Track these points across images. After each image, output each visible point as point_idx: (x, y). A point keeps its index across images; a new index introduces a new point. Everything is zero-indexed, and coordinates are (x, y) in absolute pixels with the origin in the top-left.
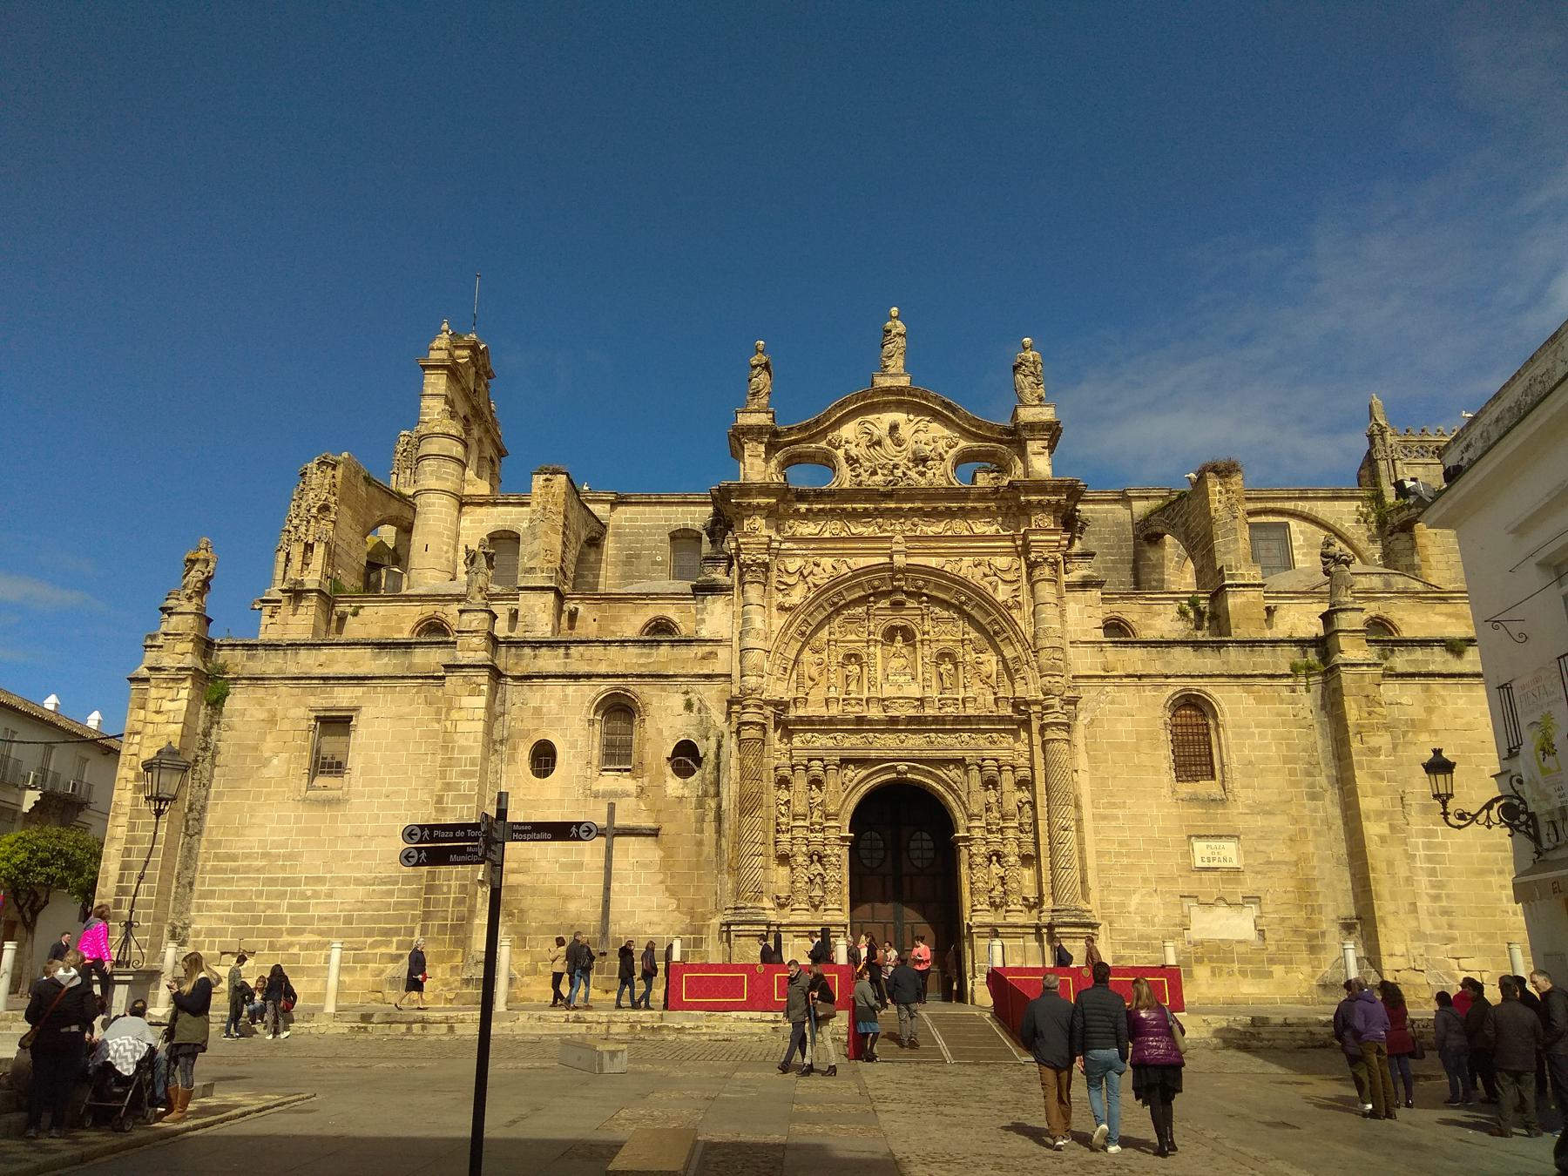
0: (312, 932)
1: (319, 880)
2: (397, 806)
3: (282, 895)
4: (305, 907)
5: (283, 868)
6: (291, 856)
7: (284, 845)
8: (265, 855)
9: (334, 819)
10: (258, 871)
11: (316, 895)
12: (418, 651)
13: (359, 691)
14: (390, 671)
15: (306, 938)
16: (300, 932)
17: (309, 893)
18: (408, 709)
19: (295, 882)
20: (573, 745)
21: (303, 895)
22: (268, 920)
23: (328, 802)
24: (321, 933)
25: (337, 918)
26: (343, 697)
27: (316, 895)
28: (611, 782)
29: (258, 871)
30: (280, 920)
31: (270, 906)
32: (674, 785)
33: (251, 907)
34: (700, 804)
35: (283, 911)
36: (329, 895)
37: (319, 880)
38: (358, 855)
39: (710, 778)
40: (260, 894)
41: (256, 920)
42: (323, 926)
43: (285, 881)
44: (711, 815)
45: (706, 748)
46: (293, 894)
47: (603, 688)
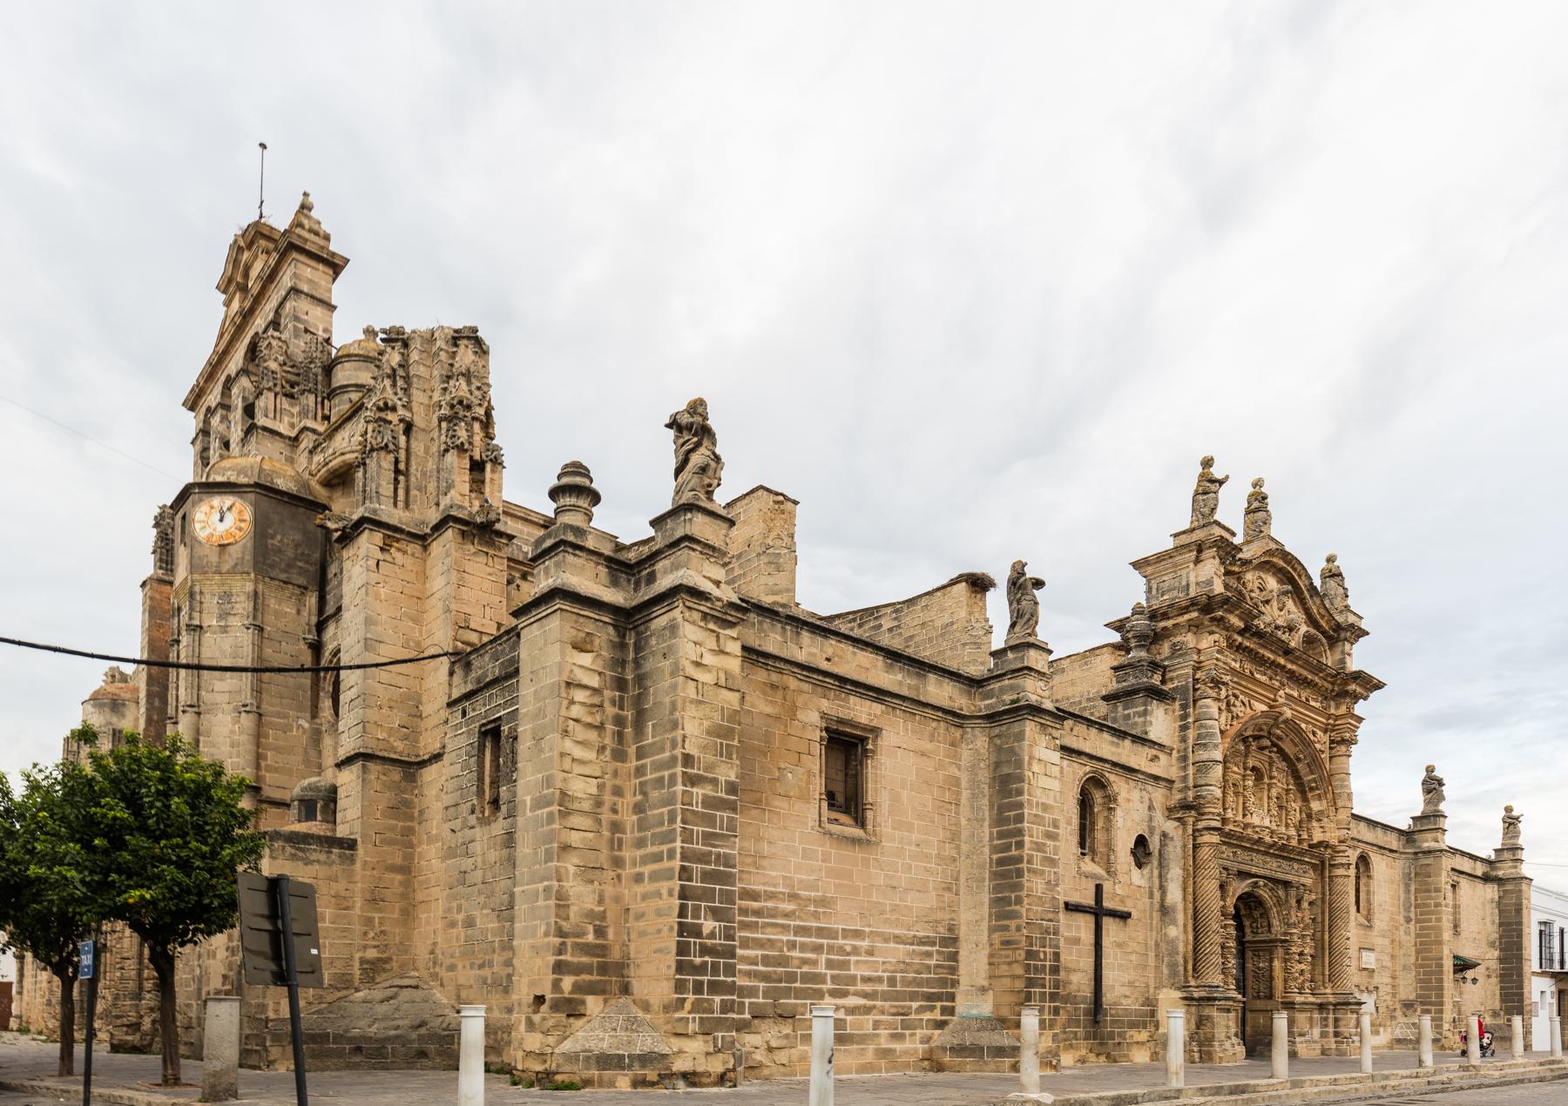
0: (856, 994)
1: (857, 934)
2: (927, 857)
3: (818, 949)
4: (844, 965)
5: (816, 915)
6: (822, 902)
7: (812, 887)
8: (793, 897)
9: (866, 862)
10: (786, 915)
11: (855, 951)
12: (932, 677)
13: (878, 708)
14: (905, 692)
15: (853, 1001)
16: (844, 994)
17: (848, 949)
18: (927, 745)
19: (831, 934)
20: (1069, 823)
21: (841, 950)
22: (808, 978)
23: (855, 841)
24: (865, 995)
25: (879, 980)
26: (862, 711)
27: (855, 951)
28: (1088, 866)
29: (786, 915)
30: (819, 978)
31: (805, 962)
32: (1138, 877)
33: (783, 961)
34: (1151, 896)
35: (821, 969)
36: (870, 953)
37: (857, 934)
38: (895, 909)
39: (1156, 872)
40: (792, 945)
41: (791, 977)
42: (868, 988)
43: (821, 932)
44: (1157, 906)
45: (1154, 844)
46: (831, 949)
47: (1088, 769)
